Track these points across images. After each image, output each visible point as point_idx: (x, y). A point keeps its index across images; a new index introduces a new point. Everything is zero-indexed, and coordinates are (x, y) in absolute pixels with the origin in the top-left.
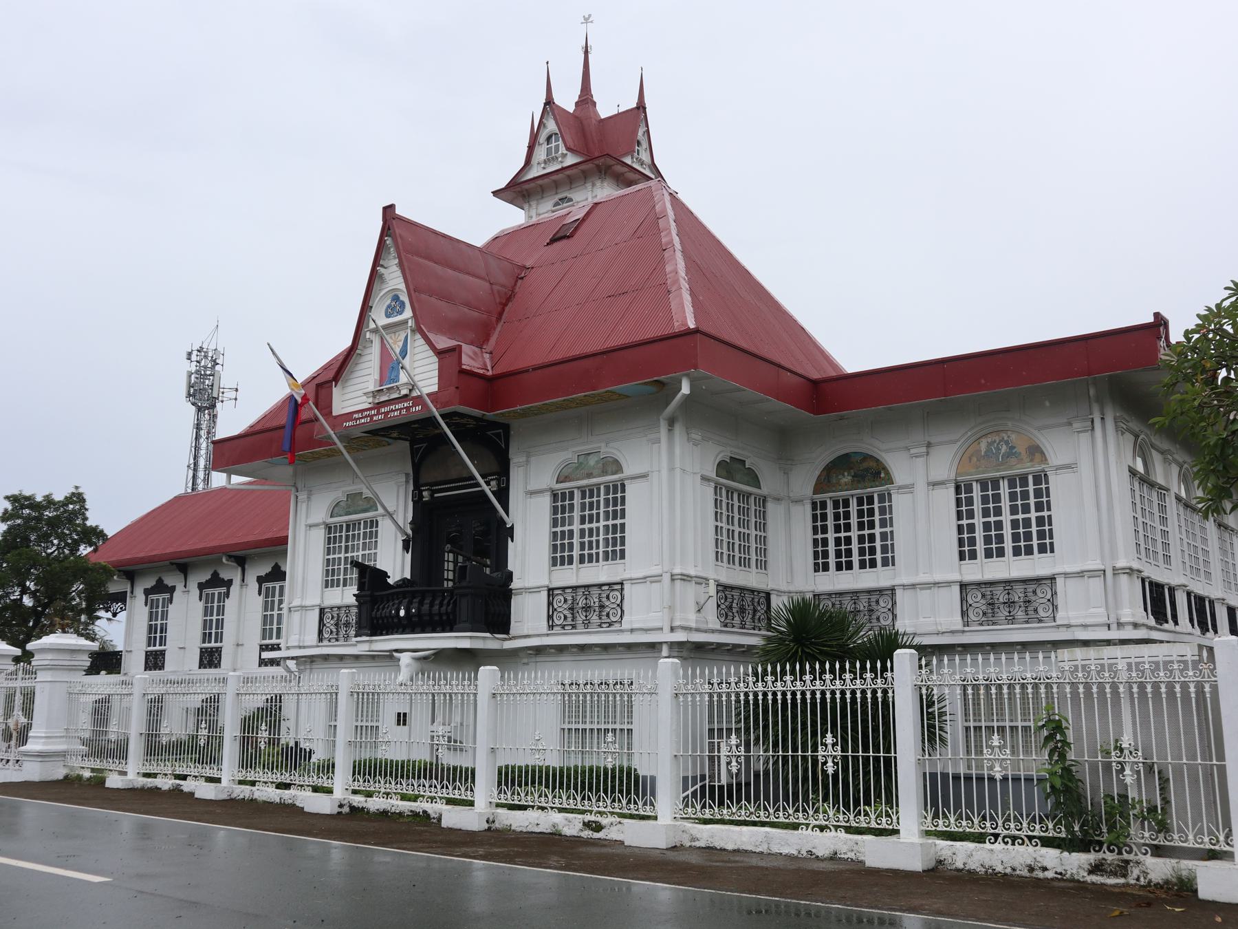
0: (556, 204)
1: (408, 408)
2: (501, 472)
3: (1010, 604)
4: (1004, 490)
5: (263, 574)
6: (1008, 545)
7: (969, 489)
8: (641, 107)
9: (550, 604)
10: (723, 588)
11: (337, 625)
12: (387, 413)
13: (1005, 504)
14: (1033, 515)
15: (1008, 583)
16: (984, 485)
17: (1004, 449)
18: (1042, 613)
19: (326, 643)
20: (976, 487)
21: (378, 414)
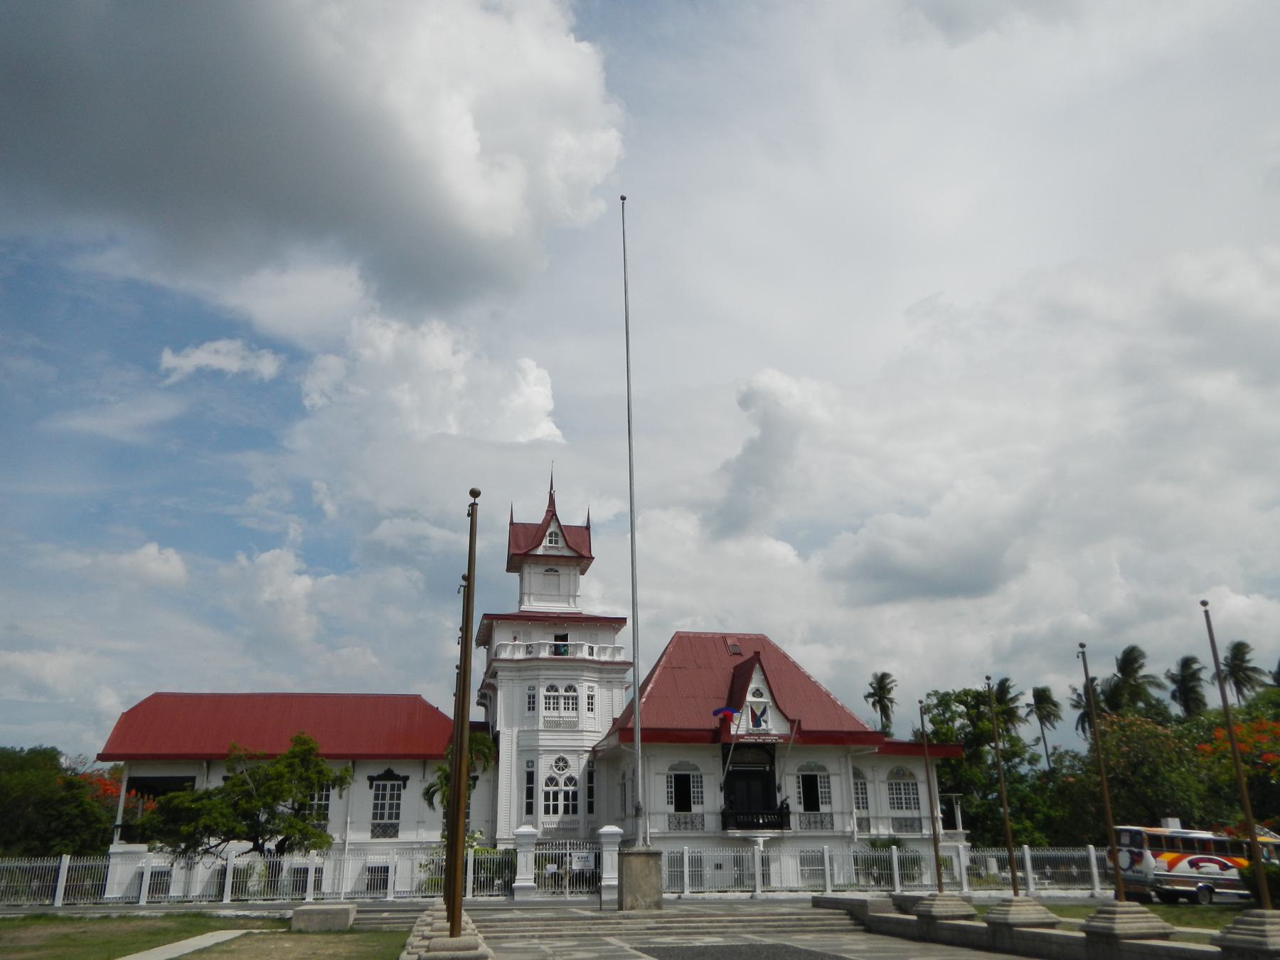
0: (547, 571)
1: (776, 740)
2: (772, 764)
3: (906, 826)
4: (902, 787)
5: (375, 774)
6: (904, 805)
7: (892, 785)
8: (588, 528)
9: (800, 820)
10: (894, 819)
11: (679, 823)
12: (764, 740)
13: (903, 792)
14: (912, 796)
15: (906, 819)
16: (896, 785)
17: (901, 772)
18: (917, 830)
19: (672, 831)
20: (902, 785)
21: (759, 738)
